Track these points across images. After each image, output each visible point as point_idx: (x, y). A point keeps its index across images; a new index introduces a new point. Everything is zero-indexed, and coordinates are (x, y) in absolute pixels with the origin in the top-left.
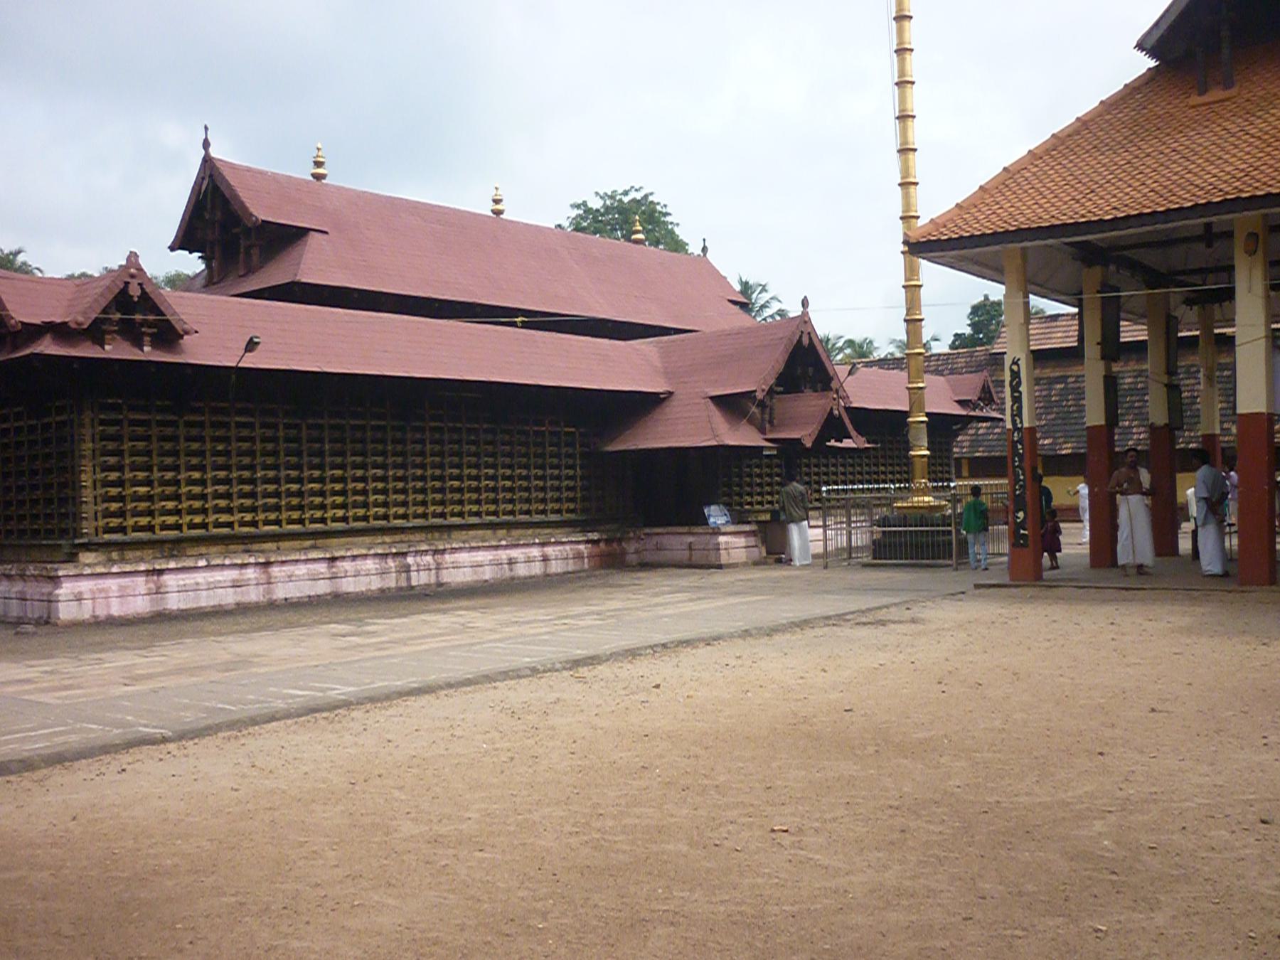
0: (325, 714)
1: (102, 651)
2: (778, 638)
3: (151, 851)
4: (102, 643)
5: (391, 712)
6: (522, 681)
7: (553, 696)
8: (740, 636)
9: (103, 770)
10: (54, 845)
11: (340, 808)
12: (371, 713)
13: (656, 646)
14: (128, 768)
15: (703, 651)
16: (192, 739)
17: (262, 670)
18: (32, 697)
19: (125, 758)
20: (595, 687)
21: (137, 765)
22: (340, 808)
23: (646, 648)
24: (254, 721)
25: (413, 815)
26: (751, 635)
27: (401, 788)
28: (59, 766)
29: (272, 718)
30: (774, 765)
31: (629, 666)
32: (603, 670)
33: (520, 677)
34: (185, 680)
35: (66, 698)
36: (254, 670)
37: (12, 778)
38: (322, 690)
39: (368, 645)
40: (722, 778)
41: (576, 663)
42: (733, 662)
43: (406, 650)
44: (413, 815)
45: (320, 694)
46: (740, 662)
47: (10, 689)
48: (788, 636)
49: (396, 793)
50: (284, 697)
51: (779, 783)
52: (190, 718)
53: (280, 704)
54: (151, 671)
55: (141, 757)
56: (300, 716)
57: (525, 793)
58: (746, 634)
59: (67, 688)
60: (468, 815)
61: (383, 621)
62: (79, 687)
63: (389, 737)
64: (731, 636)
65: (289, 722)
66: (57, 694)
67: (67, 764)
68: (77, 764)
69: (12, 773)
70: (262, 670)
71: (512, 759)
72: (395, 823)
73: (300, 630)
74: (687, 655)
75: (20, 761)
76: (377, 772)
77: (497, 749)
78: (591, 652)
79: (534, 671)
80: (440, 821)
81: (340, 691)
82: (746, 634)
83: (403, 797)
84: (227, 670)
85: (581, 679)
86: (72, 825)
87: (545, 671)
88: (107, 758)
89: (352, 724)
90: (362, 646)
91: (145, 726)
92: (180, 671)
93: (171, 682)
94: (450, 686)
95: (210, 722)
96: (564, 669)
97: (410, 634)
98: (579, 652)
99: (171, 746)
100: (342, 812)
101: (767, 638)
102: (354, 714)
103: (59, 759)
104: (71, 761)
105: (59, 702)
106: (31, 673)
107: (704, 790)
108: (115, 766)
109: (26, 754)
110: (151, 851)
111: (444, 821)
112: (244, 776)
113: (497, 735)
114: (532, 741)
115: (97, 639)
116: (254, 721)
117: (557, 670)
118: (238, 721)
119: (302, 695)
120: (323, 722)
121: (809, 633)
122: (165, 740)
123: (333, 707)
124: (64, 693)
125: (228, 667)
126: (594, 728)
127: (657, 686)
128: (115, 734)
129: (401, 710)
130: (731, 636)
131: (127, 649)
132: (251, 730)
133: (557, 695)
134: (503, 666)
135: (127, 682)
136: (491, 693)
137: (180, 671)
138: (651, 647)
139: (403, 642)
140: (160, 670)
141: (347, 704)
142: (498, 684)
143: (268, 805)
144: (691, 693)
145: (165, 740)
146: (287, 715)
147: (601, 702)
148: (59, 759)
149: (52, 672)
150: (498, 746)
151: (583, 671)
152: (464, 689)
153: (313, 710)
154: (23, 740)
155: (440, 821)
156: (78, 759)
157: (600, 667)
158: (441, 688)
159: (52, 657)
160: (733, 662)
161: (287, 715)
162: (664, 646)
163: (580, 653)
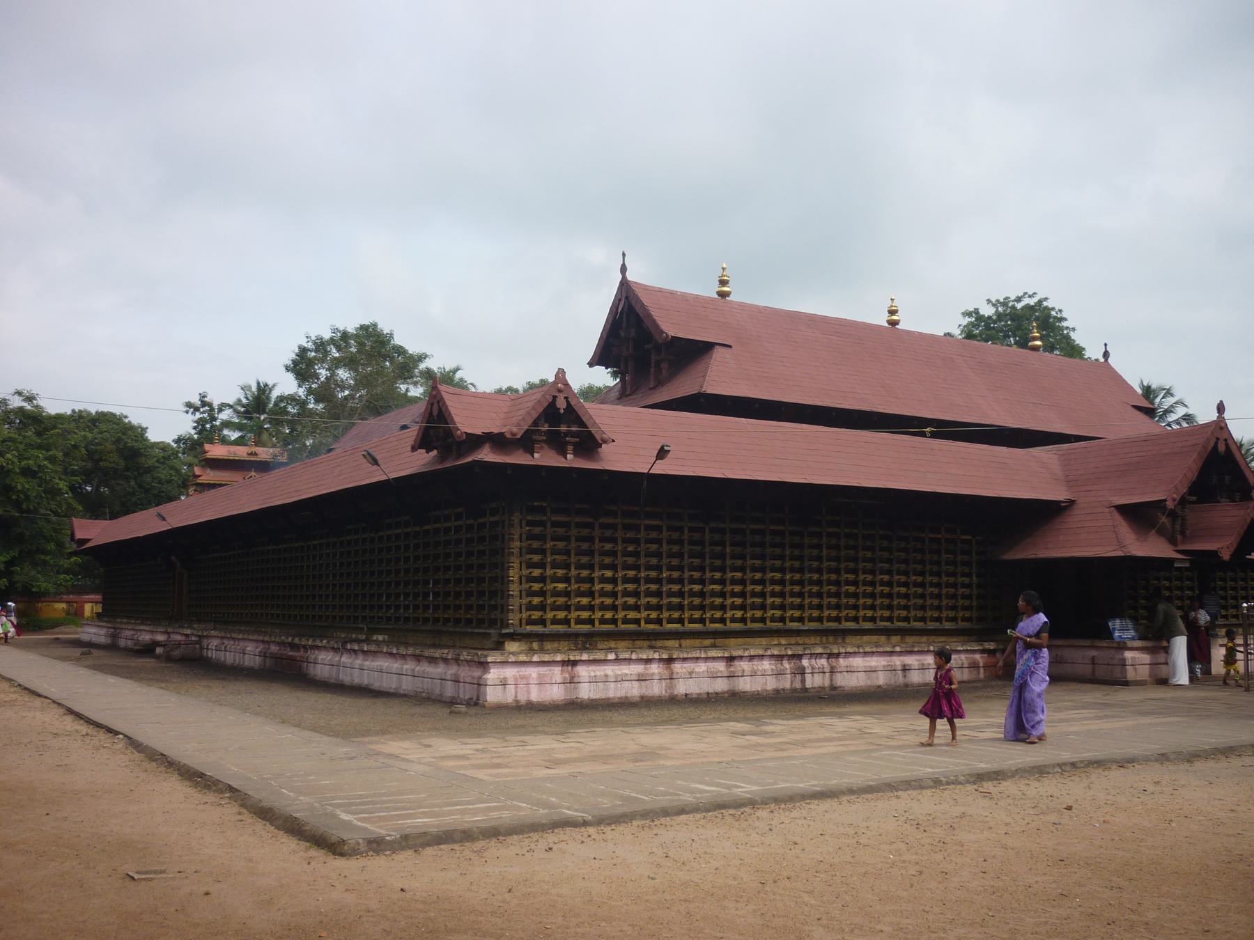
0: (732, 811)
1: (526, 734)
2: (1199, 765)
3: (578, 930)
4: (523, 726)
5: (795, 813)
6: (924, 792)
7: (958, 810)
8: (1156, 760)
9: (533, 846)
10: (493, 913)
11: (751, 907)
12: (776, 814)
13: (1065, 764)
14: (555, 847)
15: (1115, 774)
16: (610, 824)
17: (669, 763)
18: (468, 773)
19: (551, 838)
20: (1002, 803)
21: (562, 845)
22: (751, 907)
23: (1053, 766)
24: (665, 813)
25: (824, 922)
26: (1168, 759)
27: (810, 893)
28: (494, 840)
29: (682, 811)
30: (1210, 906)
31: (1037, 784)
32: (1009, 786)
33: (922, 788)
34: (600, 768)
35: (497, 775)
36: (662, 762)
37: (456, 846)
38: (729, 787)
39: (768, 745)
40: (1151, 915)
41: (980, 777)
42: (1151, 788)
43: (807, 752)
44: (824, 922)
45: (725, 791)
46: (1158, 788)
47: (450, 763)
48: (1211, 763)
49: (806, 898)
50: (692, 791)
51: (1218, 926)
52: (607, 805)
53: (688, 798)
54: (568, 756)
55: (565, 838)
56: (709, 811)
57: (937, 910)
58: (1163, 758)
59: (498, 766)
60: (879, 927)
61: (780, 722)
62: (507, 767)
63: (797, 839)
64: (1146, 759)
65: (698, 816)
66: (489, 771)
67: (501, 838)
68: (510, 839)
69: (455, 841)
70: (669, 763)
71: (921, 873)
72: (806, 928)
73: (702, 727)
74: (1097, 776)
75: (464, 832)
76: (785, 874)
77: (904, 861)
78: (995, 766)
79: (937, 783)
80: (852, 931)
81: (745, 789)
82: (1163, 758)
83: (813, 902)
84: (636, 761)
85: (986, 795)
86: (507, 896)
87: (948, 783)
88: (535, 836)
89: (757, 824)
90: (758, 745)
91: (569, 809)
92: (594, 758)
93: (587, 768)
94: (851, 791)
95: (625, 809)
96: (968, 782)
97: (807, 737)
98: (983, 765)
99: (591, 830)
100: (754, 911)
101: (1187, 765)
102: (760, 813)
103: (494, 833)
104: (505, 835)
105: (491, 779)
106: (466, 750)
107: (1132, 926)
108: (542, 845)
109: (467, 826)
110: (578, 930)
111: (856, 931)
112: (659, 866)
113: (903, 846)
114: (940, 857)
115: (520, 722)
116: (665, 813)
117: (960, 783)
118: (651, 811)
119: (708, 790)
120: (729, 819)
121: (1236, 762)
122: (585, 824)
123: (739, 804)
124: (495, 771)
125: (638, 757)
126: (1005, 847)
127: (1069, 808)
128: (542, 814)
129: (804, 813)
130: (1146, 759)
131: (546, 733)
132: (663, 820)
133: (963, 809)
134: (906, 775)
135: (547, 764)
136: (894, 801)
137: (594, 758)
138: (1060, 765)
139: (803, 744)
140: (575, 755)
141: (752, 803)
142: (900, 793)
143: (683, 897)
144: (1108, 818)
145: (585, 824)
146: (695, 809)
147: (1008, 820)
148: (494, 833)
149: (483, 751)
150: (905, 858)
151: (988, 786)
152: (866, 796)
153: (719, 806)
154: (462, 812)
155: (852, 931)
156: (510, 834)
157: (1005, 783)
158: (843, 793)
159: (479, 736)
160: (1151, 788)
161: (695, 809)
162: (1073, 765)
163: (983, 766)
